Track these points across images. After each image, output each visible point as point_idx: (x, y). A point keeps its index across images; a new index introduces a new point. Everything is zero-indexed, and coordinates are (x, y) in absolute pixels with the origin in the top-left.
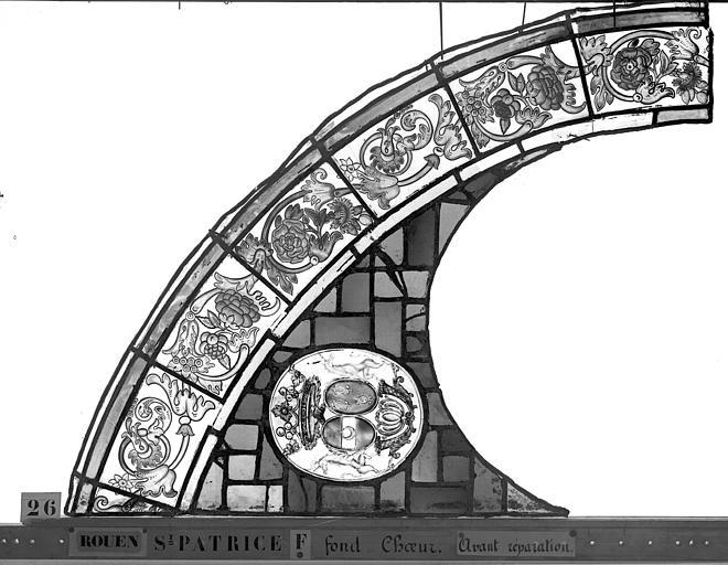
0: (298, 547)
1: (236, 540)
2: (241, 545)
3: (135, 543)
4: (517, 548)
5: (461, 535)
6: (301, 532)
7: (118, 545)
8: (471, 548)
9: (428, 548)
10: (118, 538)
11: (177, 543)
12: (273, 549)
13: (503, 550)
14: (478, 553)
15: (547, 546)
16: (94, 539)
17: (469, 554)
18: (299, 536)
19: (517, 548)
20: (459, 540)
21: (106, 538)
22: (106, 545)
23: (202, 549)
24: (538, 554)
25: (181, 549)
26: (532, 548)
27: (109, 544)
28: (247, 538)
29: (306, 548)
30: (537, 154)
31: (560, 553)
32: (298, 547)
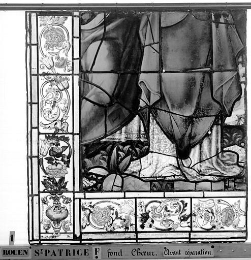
0: (96, 254)
1: (69, 251)
2: (72, 253)
3: (27, 253)
4: (189, 253)
5: (165, 248)
6: (97, 247)
7: (19, 254)
9: (151, 254)
10: (19, 251)
11: (44, 253)
14: (172, 256)
15: (201, 252)
17: (169, 256)
18: (96, 249)
19: (189, 253)
21: (14, 251)
22: (14, 254)
23: (55, 255)
24: (198, 256)
25: (46, 255)
26: (195, 253)
27: (16, 253)
28: (74, 250)
29: (99, 254)
31: (207, 255)
32: (96, 254)
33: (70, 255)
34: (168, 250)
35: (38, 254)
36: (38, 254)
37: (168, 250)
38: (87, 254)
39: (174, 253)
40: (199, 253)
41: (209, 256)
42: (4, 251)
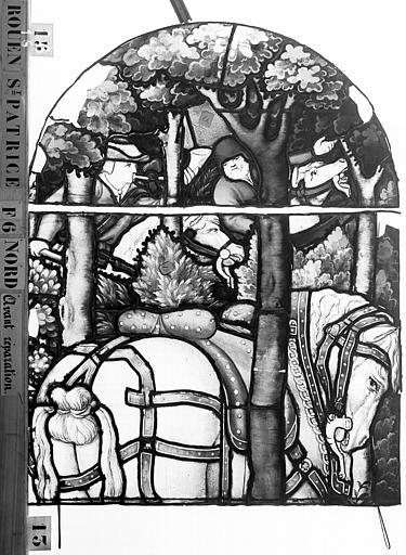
1: (16, 148)
2: (13, 152)
12: (8, 180)
13: (7, 332)
15: (9, 371)
16: (14, 255)
23: (9, 119)
25: (9, 102)
26: (8, 358)
28: (17, 157)
30: (231, 327)
31: (3, 382)
33: (8, 149)
34: (13, 303)
35: (12, 86)
36: (12, 86)
37: (13, 303)
38: (9, 183)
39: (7, 314)
41: (3, 387)
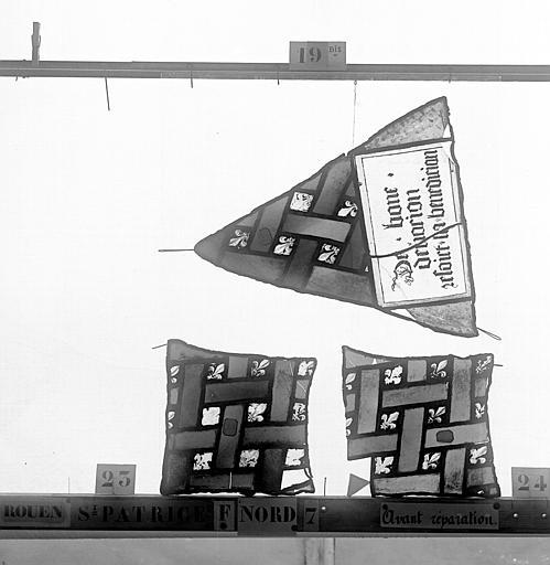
0: (222, 518)
3: (59, 515)
8: (395, 520)
19: (440, 520)
20: (382, 511)
26: (455, 520)
32: (222, 518)
34: (392, 512)
40: (464, 521)
42: (7, 508)
